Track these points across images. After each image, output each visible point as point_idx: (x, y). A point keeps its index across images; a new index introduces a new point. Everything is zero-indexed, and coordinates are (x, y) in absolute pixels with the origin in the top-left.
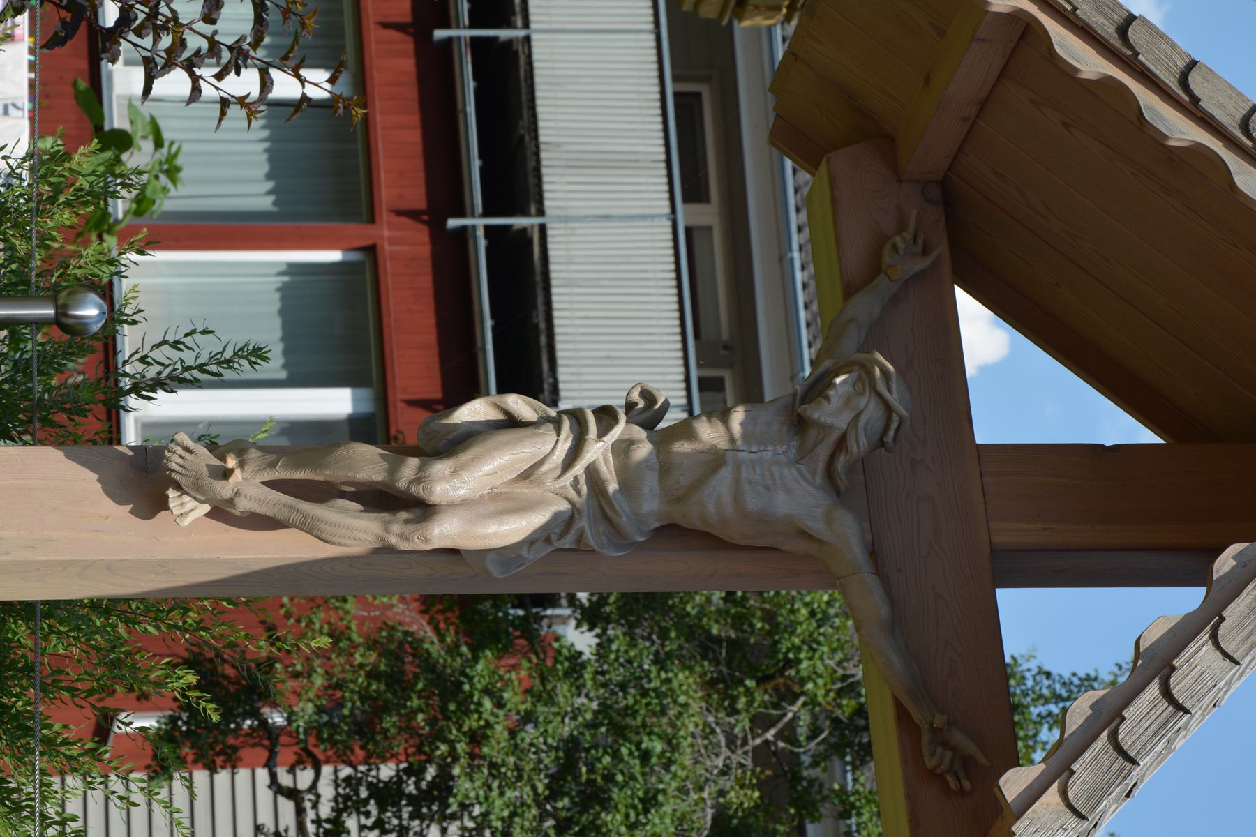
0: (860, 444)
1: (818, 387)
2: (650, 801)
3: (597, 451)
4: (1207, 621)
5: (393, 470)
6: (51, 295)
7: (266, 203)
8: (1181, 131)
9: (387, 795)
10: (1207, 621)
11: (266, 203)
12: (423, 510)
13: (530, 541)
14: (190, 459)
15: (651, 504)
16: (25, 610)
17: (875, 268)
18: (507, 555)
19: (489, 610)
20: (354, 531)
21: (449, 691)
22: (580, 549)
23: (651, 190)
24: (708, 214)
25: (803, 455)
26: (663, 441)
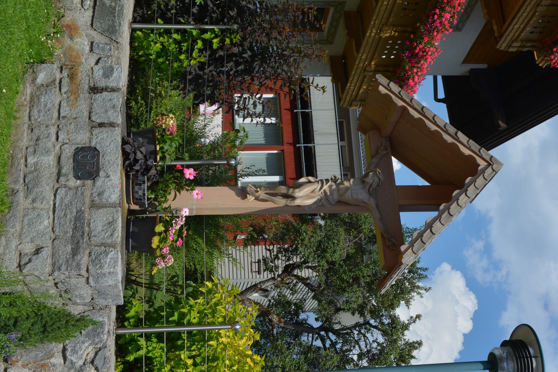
0: (374, 185)
1: (367, 175)
2: (335, 252)
3: (326, 187)
4: (439, 218)
5: (288, 191)
6: (226, 159)
7: (263, 142)
8: (433, 127)
9: (286, 250)
10: (439, 218)
11: (263, 142)
12: (293, 198)
13: (313, 204)
14: (251, 189)
15: (336, 197)
16: (222, 216)
17: (377, 153)
18: (309, 206)
19: (305, 217)
20: (281, 202)
21: (297, 232)
22: (323, 205)
23: (334, 139)
24: (345, 143)
25: (364, 187)
26: (338, 185)
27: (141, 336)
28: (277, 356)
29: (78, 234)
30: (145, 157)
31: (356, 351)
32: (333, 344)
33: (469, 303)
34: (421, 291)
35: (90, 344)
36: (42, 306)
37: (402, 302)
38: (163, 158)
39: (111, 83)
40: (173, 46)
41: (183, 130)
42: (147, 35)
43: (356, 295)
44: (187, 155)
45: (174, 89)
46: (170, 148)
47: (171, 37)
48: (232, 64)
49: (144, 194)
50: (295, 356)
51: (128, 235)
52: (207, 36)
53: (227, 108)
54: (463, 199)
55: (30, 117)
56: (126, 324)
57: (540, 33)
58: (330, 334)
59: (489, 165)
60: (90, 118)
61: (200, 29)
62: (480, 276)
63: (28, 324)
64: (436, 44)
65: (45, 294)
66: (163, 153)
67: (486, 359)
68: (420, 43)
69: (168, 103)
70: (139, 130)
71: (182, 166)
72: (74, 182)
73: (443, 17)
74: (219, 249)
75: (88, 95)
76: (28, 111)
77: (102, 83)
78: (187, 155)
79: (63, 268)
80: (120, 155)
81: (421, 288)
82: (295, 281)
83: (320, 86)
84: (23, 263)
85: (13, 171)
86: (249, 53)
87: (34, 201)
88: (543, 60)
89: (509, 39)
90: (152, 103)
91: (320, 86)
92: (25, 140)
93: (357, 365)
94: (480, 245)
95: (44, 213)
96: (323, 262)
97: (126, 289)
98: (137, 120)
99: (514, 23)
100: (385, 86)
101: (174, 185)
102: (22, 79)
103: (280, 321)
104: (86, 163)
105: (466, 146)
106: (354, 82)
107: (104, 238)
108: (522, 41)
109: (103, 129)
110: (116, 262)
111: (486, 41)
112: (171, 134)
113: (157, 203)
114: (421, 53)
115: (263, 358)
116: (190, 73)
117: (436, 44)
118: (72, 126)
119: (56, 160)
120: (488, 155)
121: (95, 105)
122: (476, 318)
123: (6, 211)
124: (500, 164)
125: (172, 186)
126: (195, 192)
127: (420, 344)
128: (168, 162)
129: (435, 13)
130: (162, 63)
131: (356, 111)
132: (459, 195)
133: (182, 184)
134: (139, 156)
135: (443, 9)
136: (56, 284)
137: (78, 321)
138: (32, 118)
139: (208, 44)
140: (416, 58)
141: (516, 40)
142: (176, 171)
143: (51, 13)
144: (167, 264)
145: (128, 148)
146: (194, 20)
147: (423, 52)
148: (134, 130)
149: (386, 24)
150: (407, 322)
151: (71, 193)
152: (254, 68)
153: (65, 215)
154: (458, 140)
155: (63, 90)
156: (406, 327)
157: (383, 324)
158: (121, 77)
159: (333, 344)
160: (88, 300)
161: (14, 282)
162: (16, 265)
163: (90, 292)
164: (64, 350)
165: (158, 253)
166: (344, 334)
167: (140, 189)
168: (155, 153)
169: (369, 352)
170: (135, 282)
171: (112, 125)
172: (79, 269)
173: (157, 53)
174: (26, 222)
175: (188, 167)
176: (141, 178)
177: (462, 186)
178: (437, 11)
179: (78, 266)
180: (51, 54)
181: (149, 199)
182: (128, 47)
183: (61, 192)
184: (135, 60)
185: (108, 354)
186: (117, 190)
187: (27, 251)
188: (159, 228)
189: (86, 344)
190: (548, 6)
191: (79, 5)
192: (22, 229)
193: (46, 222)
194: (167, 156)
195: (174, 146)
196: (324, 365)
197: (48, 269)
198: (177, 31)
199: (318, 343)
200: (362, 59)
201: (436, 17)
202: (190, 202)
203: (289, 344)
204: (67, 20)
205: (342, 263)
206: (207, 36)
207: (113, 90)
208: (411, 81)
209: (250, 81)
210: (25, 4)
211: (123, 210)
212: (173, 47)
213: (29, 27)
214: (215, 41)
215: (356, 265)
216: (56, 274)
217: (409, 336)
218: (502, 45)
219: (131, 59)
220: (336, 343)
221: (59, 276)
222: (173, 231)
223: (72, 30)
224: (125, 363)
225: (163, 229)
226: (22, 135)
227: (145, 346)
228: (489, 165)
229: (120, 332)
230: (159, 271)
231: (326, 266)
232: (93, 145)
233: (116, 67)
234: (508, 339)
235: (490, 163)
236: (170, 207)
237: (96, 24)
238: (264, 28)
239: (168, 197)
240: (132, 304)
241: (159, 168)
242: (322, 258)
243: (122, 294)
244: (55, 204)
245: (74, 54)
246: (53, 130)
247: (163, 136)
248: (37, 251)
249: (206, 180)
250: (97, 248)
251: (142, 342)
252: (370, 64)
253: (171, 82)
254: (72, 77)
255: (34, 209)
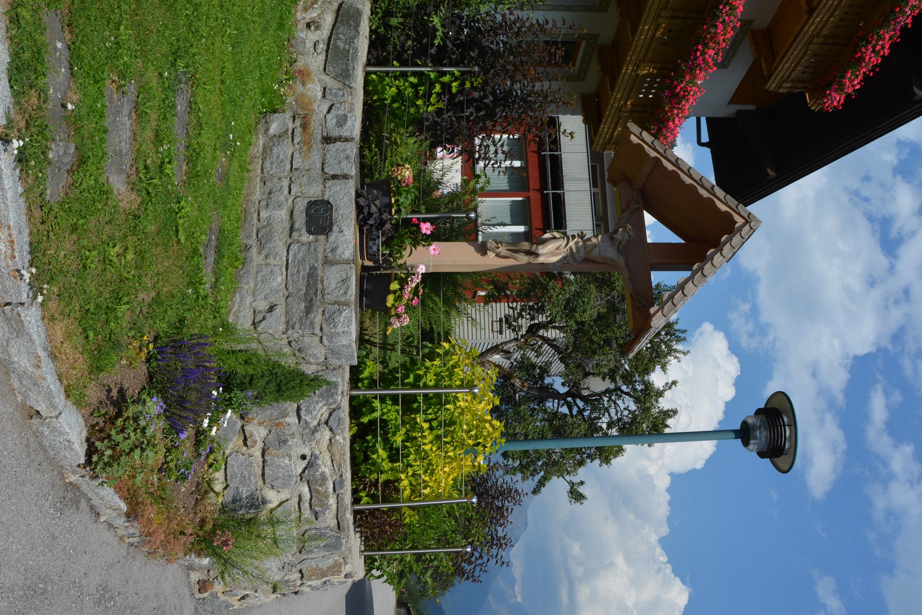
0: (624, 242)
1: (616, 231)
2: (584, 311)
3: (572, 244)
4: (691, 278)
5: (531, 247)
6: (465, 212)
7: (507, 188)
8: (688, 181)
9: (531, 308)
10: (691, 278)
11: (507, 188)
12: (537, 255)
13: (558, 262)
14: (491, 244)
15: (582, 254)
16: (461, 273)
17: (628, 207)
18: (554, 264)
19: (551, 274)
20: (524, 259)
21: (545, 288)
22: (568, 263)
23: (586, 185)
24: (598, 190)
25: (613, 244)
26: (585, 242)
27: (375, 398)
28: (520, 422)
29: (312, 292)
30: (380, 210)
31: (605, 419)
32: (581, 412)
33: (732, 367)
34: (678, 355)
35: (324, 405)
36: (276, 365)
37: (658, 367)
38: (398, 211)
39: (346, 133)
40: (410, 90)
41: (419, 181)
42: (381, 79)
43: (607, 359)
44: (423, 207)
45: (411, 136)
46: (405, 200)
47: (407, 81)
48: (472, 109)
49: (378, 250)
50: (538, 424)
51: (362, 293)
52: (446, 79)
53: (467, 157)
54: (718, 258)
55: (262, 170)
56: (360, 385)
57: (813, 73)
58: (578, 401)
59: (747, 222)
60: (323, 170)
61: (438, 72)
62: (744, 342)
63: (262, 383)
64: (699, 82)
65: (280, 354)
66: (398, 206)
67: (738, 428)
68: (682, 81)
69: (405, 152)
70: (373, 182)
71: (418, 219)
72: (306, 238)
73: (706, 53)
74: (457, 308)
75: (321, 146)
76: (260, 163)
77: (335, 133)
78: (423, 207)
79: (297, 326)
80: (354, 208)
81: (679, 352)
82: (540, 343)
83: (568, 131)
84: (257, 320)
85: (247, 225)
86: (491, 98)
87: (267, 257)
88: (815, 103)
89: (778, 78)
90: (386, 151)
91: (568, 131)
92: (258, 193)
93: (607, 434)
94: (746, 307)
95: (276, 269)
96: (572, 322)
97: (359, 348)
98: (371, 169)
99: (784, 62)
100: (638, 135)
101: (410, 240)
102: (255, 129)
103: (523, 386)
104: (319, 218)
105: (723, 202)
106: (608, 123)
107: (337, 296)
108: (793, 81)
109: (336, 181)
110: (350, 321)
111: (753, 81)
112: (407, 186)
113: (391, 259)
114: (682, 93)
115: (503, 424)
116: (427, 120)
117: (699, 82)
118: (305, 179)
119: (288, 213)
120: (746, 211)
121: (328, 156)
122: (738, 383)
123: (240, 267)
124: (759, 222)
125: (408, 242)
126: (432, 248)
127: (675, 412)
128: (403, 216)
129: (698, 50)
130: (398, 108)
131: (609, 154)
132: (714, 254)
133: (419, 239)
134: (374, 209)
135: (706, 45)
136: (290, 343)
137: (312, 380)
138: (265, 170)
139: (446, 87)
140: (676, 98)
141: (786, 80)
142: (412, 225)
143: (283, 59)
144: (402, 323)
145: (362, 201)
146: (432, 62)
147: (685, 92)
148: (368, 181)
149: (644, 60)
150: (662, 389)
151: (304, 249)
152: (496, 114)
153: (298, 272)
154: (714, 195)
155: (295, 141)
156: (660, 394)
157: (635, 390)
158: (354, 126)
159: (581, 412)
160: (322, 359)
161: (249, 339)
162: (250, 322)
163: (323, 351)
164: (298, 410)
165: (393, 312)
166: (594, 401)
167: (374, 244)
168: (390, 206)
169: (619, 420)
170: (368, 341)
171: (345, 177)
172: (313, 328)
173: (392, 97)
174: (259, 279)
175: (425, 220)
176: (375, 233)
177: (718, 246)
178: (700, 47)
179: (312, 324)
180: (283, 102)
181: (383, 255)
182: (362, 92)
183: (294, 248)
184: (369, 105)
185: (342, 415)
186: (351, 246)
187: (261, 308)
188: (395, 286)
189: (320, 405)
190: (821, 44)
191: (312, 49)
192: (256, 286)
193: (279, 279)
194: (403, 210)
195: (410, 198)
196: (571, 433)
197: (282, 327)
198: (414, 74)
199: (564, 410)
200: (617, 99)
201: (698, 54)
202: (428, 258)
203: (534, 409)
204: (299, 65)
205: (592, 323)
206: (446, 79)
207: (347, 140)
208: (671, 123)
209: (491, 128)
210: (258, 52)
211: (356, 266)
212: (409, 92)
213: (262, 75)
214: (454, 84)
215: (608, 326)
216: (290, 332)
217: (664, 404)
218: (772, 86)
219: (365, 103)
220: (584, 410)
221: (293, 334)
222: (408, 289)
223: (304, 75)
224: (360, 425)
225: (398, 287)
226: (255, 188)
227: (379, 408)
228: (747, 222)
229: (354, 393)
230: (394, 331)
231: (575, 327)
232: (326, 198)
233: (350, 115)
234: (762, 406)
235: (748, 219)
236: (405, 263)
237: (330, 69)
238: (507, 70)
239: (404, 253)
240: (366, 365)
241: (393, 222)
242: (570, 318)
243: (356, 354)
244: (287, 261)
245: (306, 101)
246: (286, 183)
247: (398, 188)
248: (271, 309)
249: (444, 235)
250: (330, 306)
251: (377, 403)
252: (625, 104)
253: (407, 128)
254: (305, 126)
255: (267, 265)
